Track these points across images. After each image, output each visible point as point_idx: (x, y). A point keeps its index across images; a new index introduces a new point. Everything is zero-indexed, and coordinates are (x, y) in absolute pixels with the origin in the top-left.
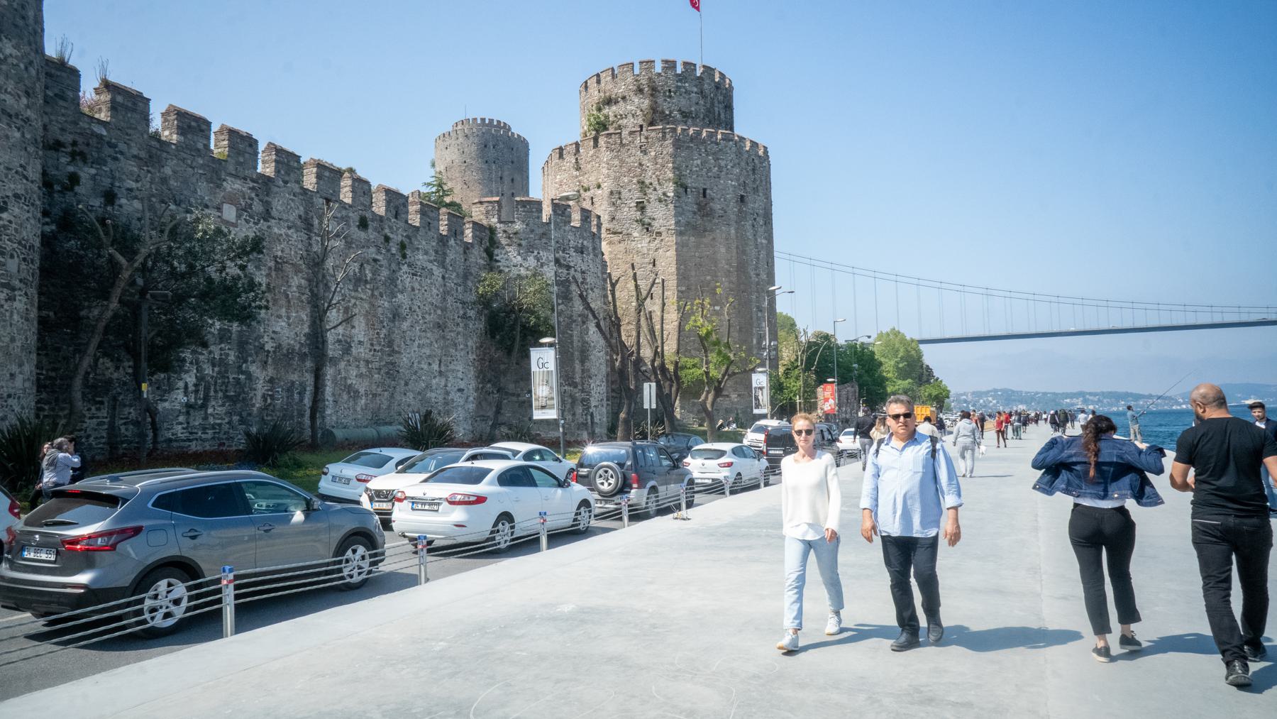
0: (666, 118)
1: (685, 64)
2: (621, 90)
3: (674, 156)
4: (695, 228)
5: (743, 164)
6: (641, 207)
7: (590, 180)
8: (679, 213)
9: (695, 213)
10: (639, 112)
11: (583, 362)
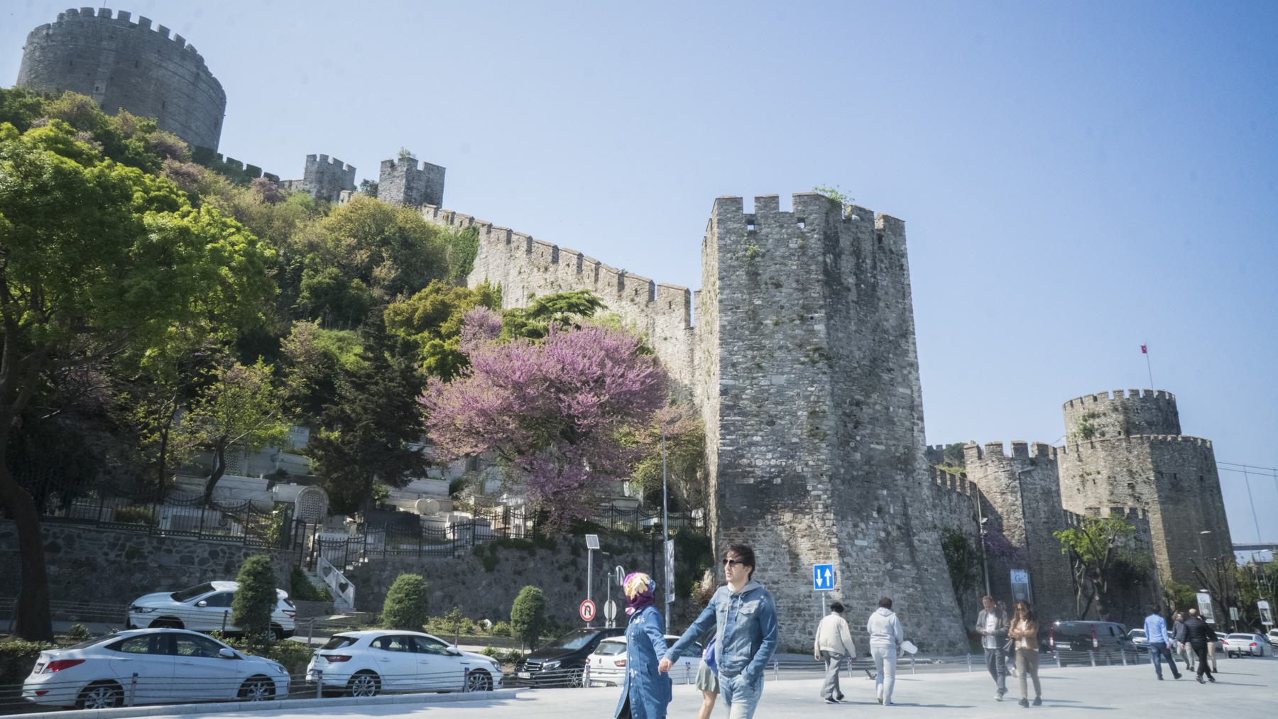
0: (1139, 429)
1: (1146, 391)
2: (1100, 408)
3: (1152, 454)
4: (1172, 499)
5: (1198, 455)
6: (1131, 486)
7: (1092, 468)
8: (1159, 490)
9: (1170, 490)
10: (1116, 423)
11: (1155, 591)
